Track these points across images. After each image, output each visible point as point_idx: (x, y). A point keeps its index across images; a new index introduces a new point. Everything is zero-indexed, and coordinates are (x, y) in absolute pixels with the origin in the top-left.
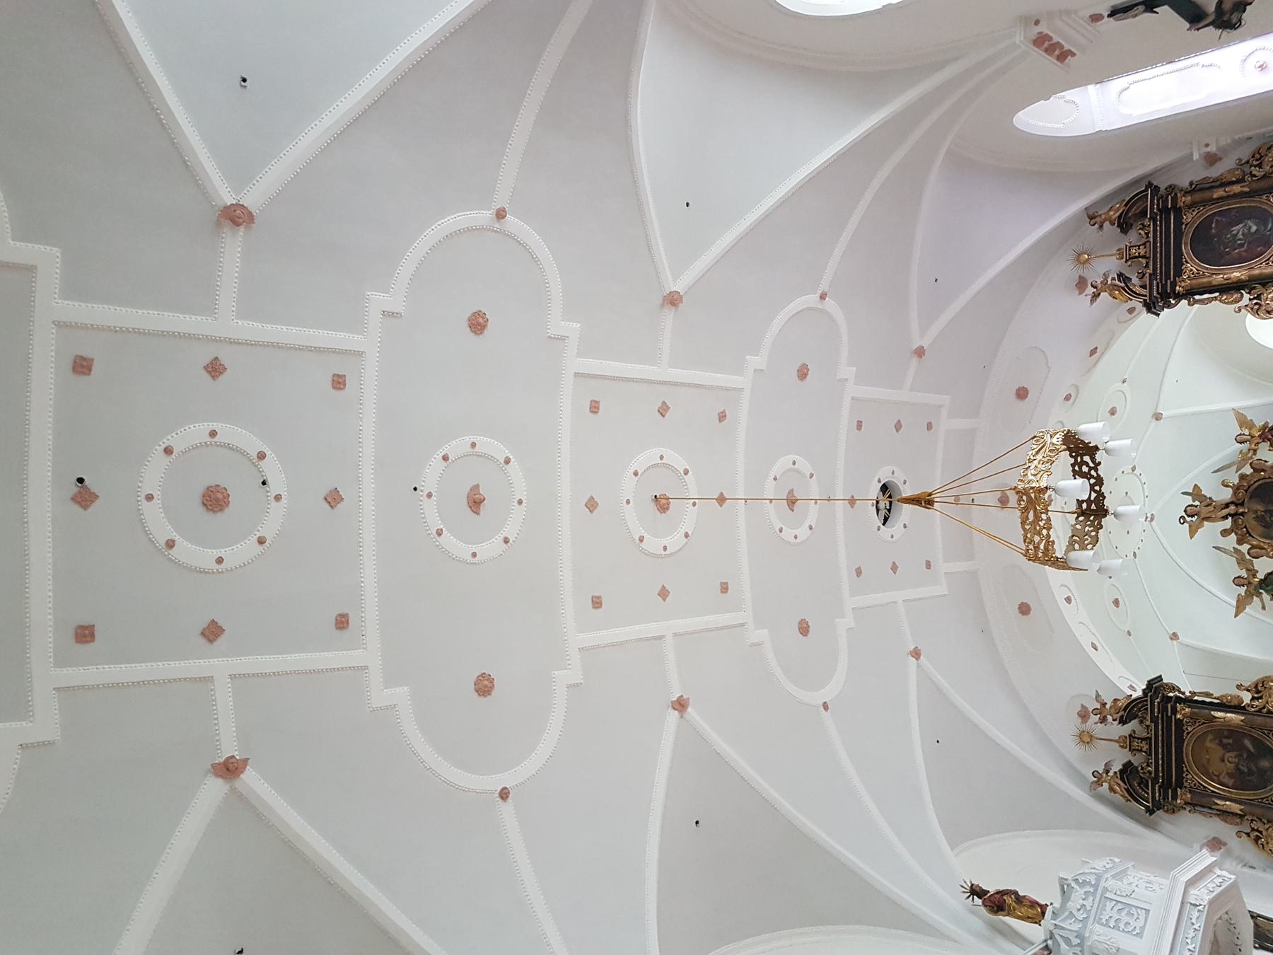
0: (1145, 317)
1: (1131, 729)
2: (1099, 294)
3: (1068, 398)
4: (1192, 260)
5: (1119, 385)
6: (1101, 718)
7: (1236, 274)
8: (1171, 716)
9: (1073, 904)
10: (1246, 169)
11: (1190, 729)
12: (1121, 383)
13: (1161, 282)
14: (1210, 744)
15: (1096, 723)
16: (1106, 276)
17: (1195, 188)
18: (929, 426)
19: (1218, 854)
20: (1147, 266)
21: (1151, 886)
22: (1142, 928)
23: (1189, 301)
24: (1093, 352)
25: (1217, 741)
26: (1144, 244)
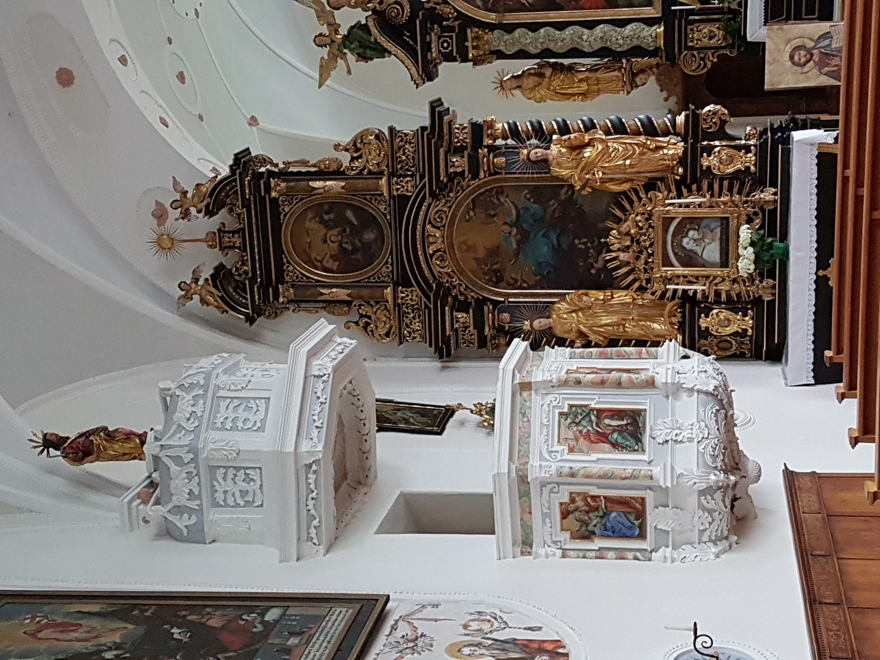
1: (219, 221)
6: (183, 211)
8: (265, 196)
11: (287, 210)
14: (312, 225)
15: (177, 219)
21: (268, 373)
22: (264, 421)
25: (317, 219)
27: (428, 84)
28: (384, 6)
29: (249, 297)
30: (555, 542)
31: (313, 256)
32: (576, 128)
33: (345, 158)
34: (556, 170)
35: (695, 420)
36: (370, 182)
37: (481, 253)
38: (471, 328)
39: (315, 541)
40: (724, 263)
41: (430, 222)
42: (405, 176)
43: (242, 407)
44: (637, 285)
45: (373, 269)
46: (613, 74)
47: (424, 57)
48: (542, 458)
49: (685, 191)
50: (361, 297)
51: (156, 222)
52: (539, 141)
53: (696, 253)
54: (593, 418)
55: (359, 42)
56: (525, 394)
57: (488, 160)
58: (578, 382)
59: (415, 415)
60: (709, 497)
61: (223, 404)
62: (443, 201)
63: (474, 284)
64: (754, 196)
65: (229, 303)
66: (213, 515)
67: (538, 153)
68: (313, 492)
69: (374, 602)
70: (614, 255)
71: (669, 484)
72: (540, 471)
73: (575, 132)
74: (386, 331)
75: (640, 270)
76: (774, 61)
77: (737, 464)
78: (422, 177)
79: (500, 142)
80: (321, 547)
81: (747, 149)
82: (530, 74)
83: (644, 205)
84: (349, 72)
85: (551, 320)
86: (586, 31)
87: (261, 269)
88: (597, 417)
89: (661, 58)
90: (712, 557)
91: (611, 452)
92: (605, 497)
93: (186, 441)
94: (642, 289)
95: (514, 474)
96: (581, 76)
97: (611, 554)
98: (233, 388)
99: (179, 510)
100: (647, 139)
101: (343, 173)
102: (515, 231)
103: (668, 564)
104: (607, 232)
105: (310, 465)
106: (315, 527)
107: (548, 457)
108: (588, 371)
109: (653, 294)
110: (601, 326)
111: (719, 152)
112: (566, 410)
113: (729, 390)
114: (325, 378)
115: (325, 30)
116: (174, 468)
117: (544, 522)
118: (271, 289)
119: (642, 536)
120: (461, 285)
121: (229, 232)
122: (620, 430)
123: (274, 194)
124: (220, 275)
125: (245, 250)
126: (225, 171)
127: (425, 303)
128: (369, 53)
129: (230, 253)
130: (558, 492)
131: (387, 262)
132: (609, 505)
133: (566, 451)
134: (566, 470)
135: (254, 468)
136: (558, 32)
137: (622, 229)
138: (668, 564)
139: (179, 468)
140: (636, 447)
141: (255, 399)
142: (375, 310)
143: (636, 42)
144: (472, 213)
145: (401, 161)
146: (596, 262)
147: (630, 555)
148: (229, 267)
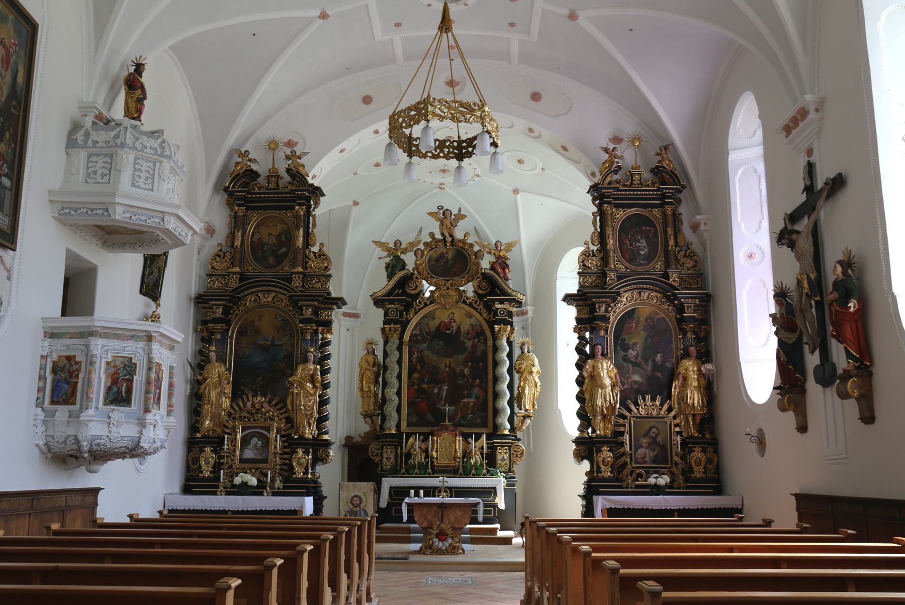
0: (588, 184)
2: (607, 153)
3: (531, 130)
4: (625, 214)
5: (541, 165)
7: (611, 242)
9: (144, 139)
10: (684, 248)
11: (289, 214)
12: (541, 167)
13: (612, 195)
16: (621, 157)
17: (676, 217)
18: (512, 25)
19: (204, 232)
20: (624, 185)
22: (138, 187)
23: (596, 213)
24: (564, 148)
26: (641, 184)
27: (372, 302)
28: (415, 279)
29: (240, 189)
30: (51, 352)
31: (261, 228)
32: (325, 379)
33: (315, 249)
34: (300, 368)
35: (122, 434)
36: (301, 262)
37: (257, 324)
38: (213, 316)
39: (61, 212)
40: (242, 461)
41: (276, 295)
42: (303, 282)
43: (148, 175)
44: (232, 412)
45: (252, 261)
46: (372, 405)
47: (386, 300)
48: (103, 346)
49: (284, 439)
50: (235, 253)
51: (286, 141)
52: (319, 358)
53: (248, 446)
54: (128, 377)
55: (396, 265)
56: (145, 338)
57: (308, 329)
58: (150, 369)
59: (155, 279)
60: (73, 441)
61: (151, 165)
62: (288, 303)
63: (239, 319)
64: (279, 477)
65: (236, 178)
66: (83, 154)
67: (311, 357)
68: (91, 212)
69: (11, 242)
70: (251, 399)
71: (82, 418)
72: (95, 344)
73: (322, 379)
74: (215, 267)
75: (241, 413)
76: (355, 487)
77: (98, 459)
78: (301, 291)
79: (320, 336)
80: (57, 215)
81: (306, 473)
82: (375, 360)
83: (278, 417)
84: (380, 258)
85: (215, 362)
86: (396, 390)
87: (255, 197)
88: (128, 380)
89: (379, 432)
90: (37, 442)
91: (105, 386)
92: (77, 382)
93: (129, 142)
94: (230, 415)
95: (94, 329)
96: (372, 387)
97: (41, 384)
98: (161, 171)
99: (87, 135)
100: (315, 418)
101: (307, 247)
102: (268, 343)
103: (33, 417)
104: (264, 395)
105: (107, 212)
106: (70, 212)
107: (104, 350)
108: (160, 376)
109: (227, 421)
110: (209, 390)
111: (305, 458)
112: (133, 361)
113: (146, 457)
114: (162, 223)
115: (403, 246)
116: (112, 134)
117: (64, 346)
118: (242, 202)
119: (53, 402)
120: (239, 311)
121: (277, 181)
122: (119, 392)
123: (297, 207)
124: (253, 175)
125: (267, 189)
126: (310, 180)
127: (229, 290)
128: (390, 270)
129: (266, 181)
130: (82, 355)
131: (255, 269)
132: (73, 384)
133: (108, 360)
134: (94, 359)
135: (109, 179)
136: (396, 375)
137: (264, 403)
138: (33, 417)
139: (112, 136)
140: (107, 401)
141: (153, 183)
142: (228, 261)
143: (388, 418)
144: (280, 319)
145: (312, 280)
146: (248, 389)
147: (40, 395)
148: (258, 180)
